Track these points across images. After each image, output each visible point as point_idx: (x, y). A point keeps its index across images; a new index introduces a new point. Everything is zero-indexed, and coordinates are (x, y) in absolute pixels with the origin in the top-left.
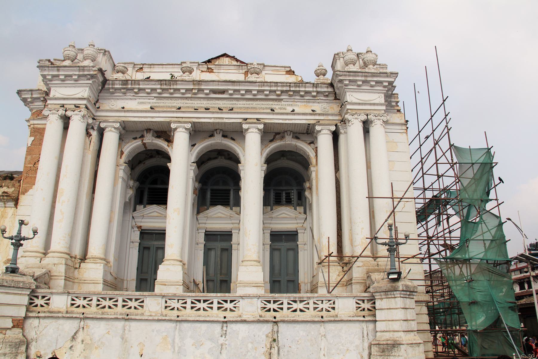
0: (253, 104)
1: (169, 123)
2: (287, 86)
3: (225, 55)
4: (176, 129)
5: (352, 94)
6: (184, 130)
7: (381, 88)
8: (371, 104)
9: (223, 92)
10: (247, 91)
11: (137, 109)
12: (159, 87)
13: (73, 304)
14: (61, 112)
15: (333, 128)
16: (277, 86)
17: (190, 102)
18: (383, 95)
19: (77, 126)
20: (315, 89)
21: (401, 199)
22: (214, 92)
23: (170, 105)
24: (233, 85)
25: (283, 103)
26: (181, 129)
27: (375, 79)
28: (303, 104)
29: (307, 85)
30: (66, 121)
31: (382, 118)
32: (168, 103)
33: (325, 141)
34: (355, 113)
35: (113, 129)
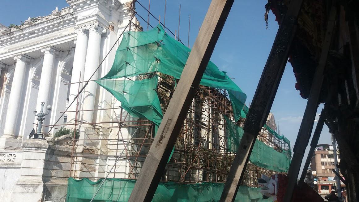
0: (48, 36)
1: (13, 57)
2: (58, 19)
4: (16, 60)
7: (95, 4)
8: (89, 17)
9: (34, 33)
10: (43, 28)
12: (8, 37)
16: (54, 21)
18: (97, 9)
20: (72, 17)
21: (88, 81)
24: (35, 27)
28: (70, 28)
29: (68, 15)
31: (93, 26)
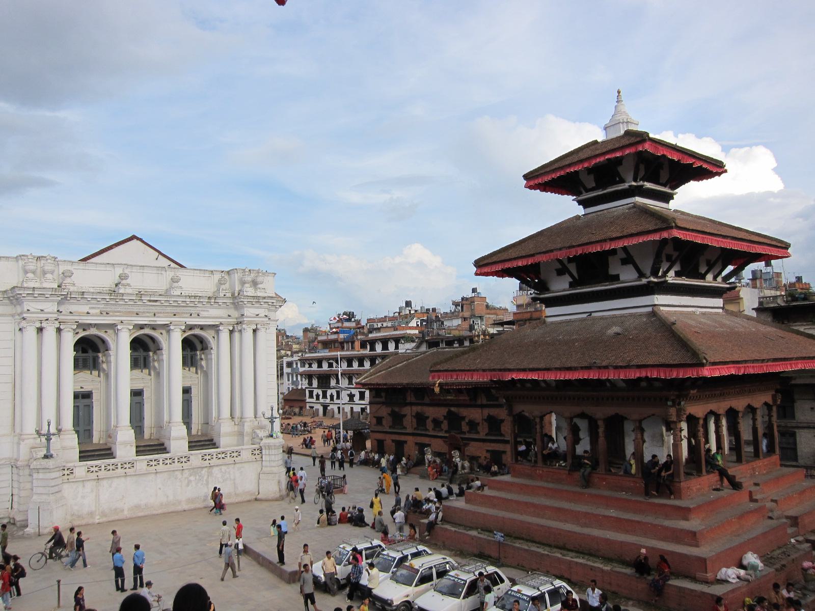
3: (133, 238)
5: (249, 309)
6: (127, 330)
11: (91, 314)
13: (88, 471)
14: (38, 325)
15: (231, 328)
17: (131, 307)
19: (50, 333)
22: (150, 301)
23: (116, 310)
25: (198, 309)
26: (125, 330)
27: (265, 301)
30: (40, 330)
32: (113, 308)
33: (224, 336)
34: (250, 323)
35: (70, 330)
